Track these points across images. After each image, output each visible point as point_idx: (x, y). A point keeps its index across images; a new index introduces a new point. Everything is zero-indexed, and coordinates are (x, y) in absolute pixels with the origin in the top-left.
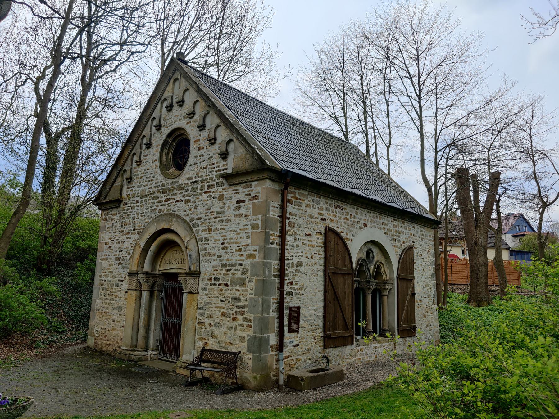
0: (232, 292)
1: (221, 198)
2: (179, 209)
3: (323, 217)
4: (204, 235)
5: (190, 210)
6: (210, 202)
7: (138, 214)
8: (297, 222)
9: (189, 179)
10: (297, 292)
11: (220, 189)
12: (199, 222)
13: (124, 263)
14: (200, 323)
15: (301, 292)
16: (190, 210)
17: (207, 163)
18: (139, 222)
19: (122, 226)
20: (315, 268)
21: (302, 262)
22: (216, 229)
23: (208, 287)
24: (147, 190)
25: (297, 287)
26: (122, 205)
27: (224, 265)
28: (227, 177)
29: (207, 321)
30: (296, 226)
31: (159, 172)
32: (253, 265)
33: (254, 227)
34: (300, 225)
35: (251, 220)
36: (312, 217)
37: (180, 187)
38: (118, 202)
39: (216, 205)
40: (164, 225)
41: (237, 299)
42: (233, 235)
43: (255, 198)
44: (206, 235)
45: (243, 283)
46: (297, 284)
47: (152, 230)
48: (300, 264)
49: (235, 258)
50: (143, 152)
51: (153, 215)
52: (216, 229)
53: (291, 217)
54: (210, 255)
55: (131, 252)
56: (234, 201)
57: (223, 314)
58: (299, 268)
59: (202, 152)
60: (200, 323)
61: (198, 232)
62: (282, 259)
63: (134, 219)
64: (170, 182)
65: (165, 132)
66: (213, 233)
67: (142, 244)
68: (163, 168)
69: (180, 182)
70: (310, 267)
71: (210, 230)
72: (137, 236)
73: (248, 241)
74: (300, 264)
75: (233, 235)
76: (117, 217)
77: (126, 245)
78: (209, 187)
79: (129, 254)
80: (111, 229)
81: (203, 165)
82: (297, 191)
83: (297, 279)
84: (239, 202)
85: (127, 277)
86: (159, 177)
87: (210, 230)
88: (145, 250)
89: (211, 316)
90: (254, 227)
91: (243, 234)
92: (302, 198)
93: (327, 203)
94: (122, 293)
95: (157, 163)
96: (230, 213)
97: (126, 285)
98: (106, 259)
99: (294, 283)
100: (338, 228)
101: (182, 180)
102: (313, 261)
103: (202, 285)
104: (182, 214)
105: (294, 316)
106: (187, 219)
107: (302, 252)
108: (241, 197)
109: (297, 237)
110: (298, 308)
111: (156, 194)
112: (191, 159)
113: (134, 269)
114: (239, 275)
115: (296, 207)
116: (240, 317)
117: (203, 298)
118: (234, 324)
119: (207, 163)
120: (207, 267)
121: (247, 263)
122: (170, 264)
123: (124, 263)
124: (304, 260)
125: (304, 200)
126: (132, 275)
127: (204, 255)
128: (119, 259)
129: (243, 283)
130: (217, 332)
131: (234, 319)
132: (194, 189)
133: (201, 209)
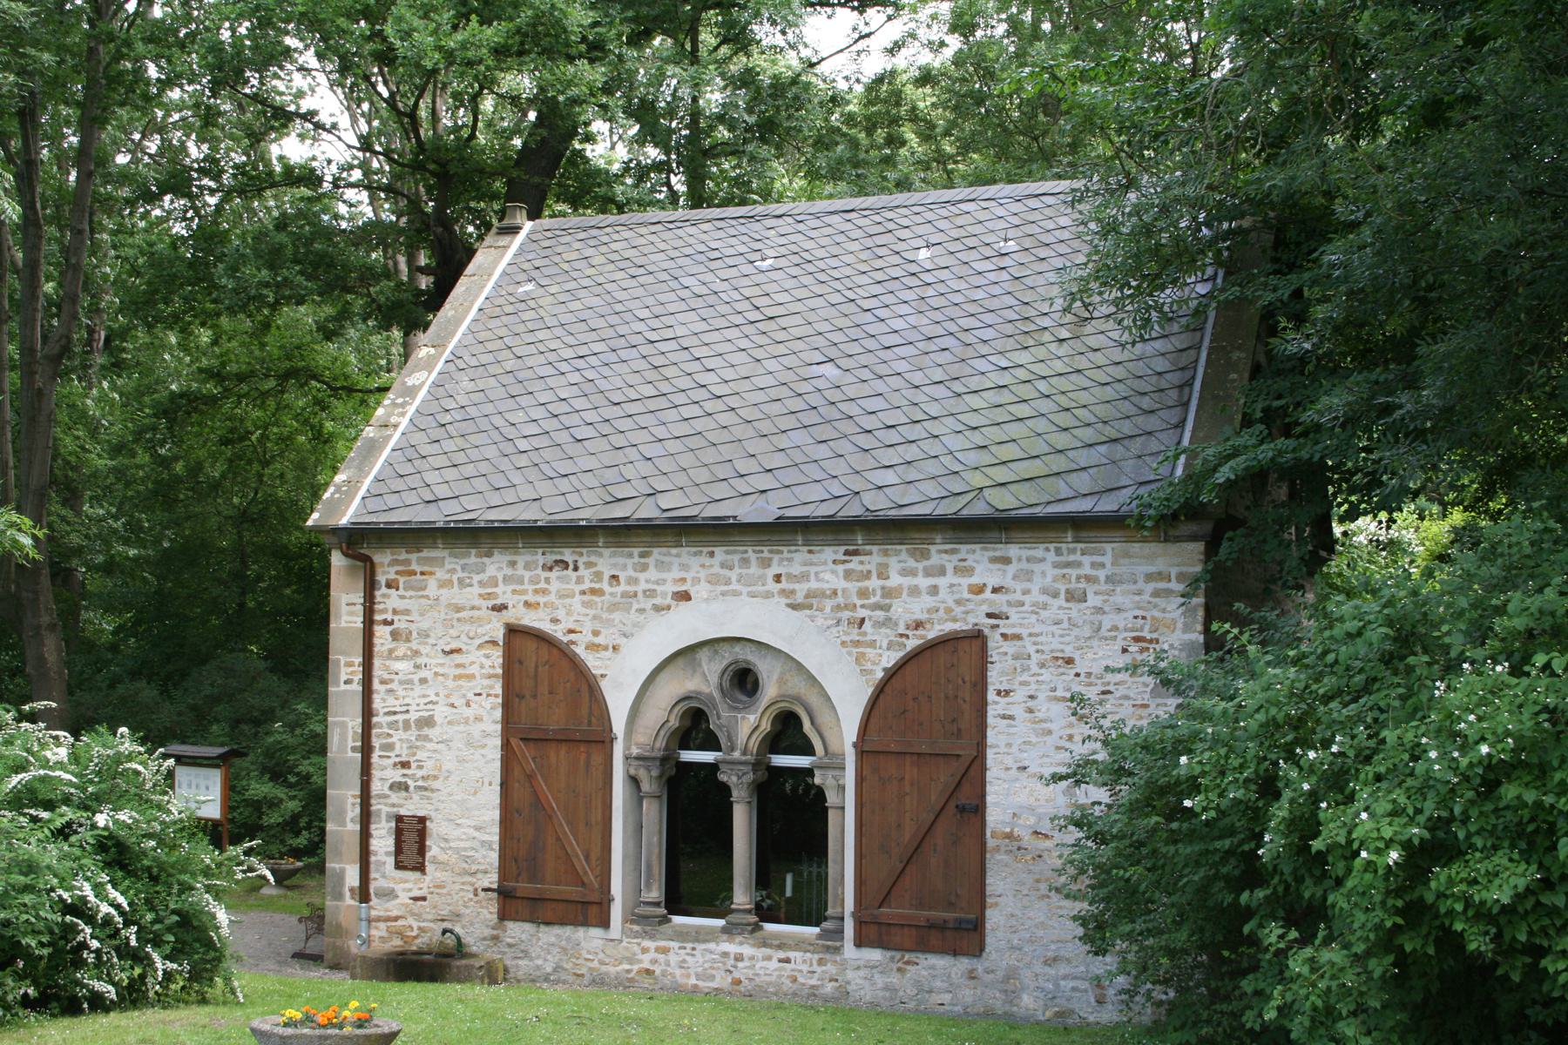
3: (498, 602)
8: (413, 627)
10: (420, 783)
15: (435, 784)
20: (476, 730)
21: (432, 717)
25: (420, 773)
30: (415, 635)
34: (425, 635)
36: (459, 609)
46: (421, 767)
48: (428, 722)
53: (396, 618)
58: (426, 731)
62: (368, 713)
70: (462, 728)
74: (428, 722)
82: (414, 557)
83: (421, 755)
92: (426, 569)
93: (513, 564)
99: (414, 765)
100: (555, 621)
102: (469, 713)
105: (410, 838)
107: (437, 694)
109: (419, 661)
110: (422, 820)
115: (411, 593)
124: (441, 712)
125: (431, 573)
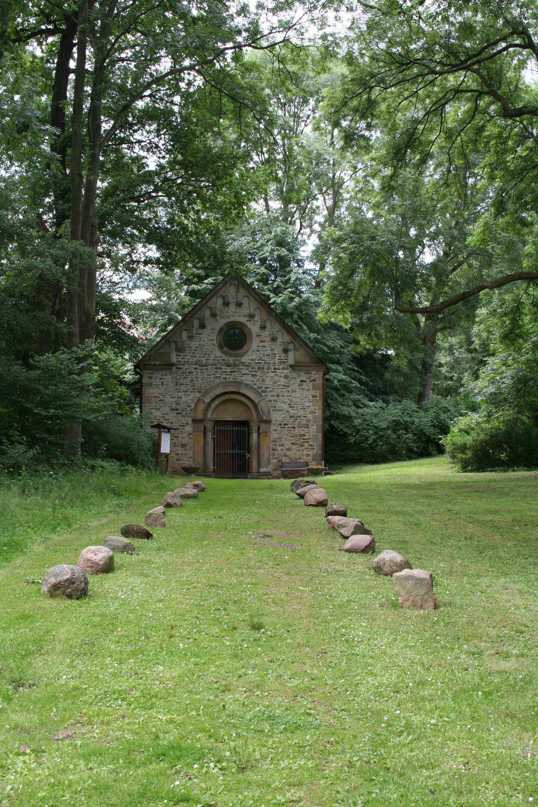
0: (297, 431)
1: (286, 377)
2: (248, 379)
4: (272, 398)
5: (258, 381)
6: (276, 378)
7: (197, 378)
9: (252, 360)
11: (285, 371)
12: (268, 390)
13: (184, 413)
14: (273, 450)
16: (258, 381)
17: (269, 352)
18: (199, 383)
19: (177, 385)
22: (283, 396)
23: (279, 429)
24: (204, 361)
26: (174, 369)
27: (293, 417)
28: (291, 366)
29: (279, 448)
31: (217, 349)
32: (314, 417)
33: (314, 396)
35: (312, 392)
37: (243, 364)
38: (169, 366)
39: (283, 381)
40: (230, 389)
41: (304, 435)
42: (298, 400)
43: (314, 380)
44: (275, 398)
45: (307, 426)
47: (218, 392)
49: (301, 413)
50: (195, 331)
51: (217, 381)
52: (283, 396)
54: (279, 410)
55: (193, 405)
56: (298, 380)
57: (293, 444)
59: (266, 344)
60: (273, 450)
61: (266, 396)
63: (192, 381)
64: (231, 359)
65: (222, 322)
66: (281, 398)
67: (207, 401)
68: (221, 347)
69: (243, 360)
71: (278, 396)
72: (198, 395)
73: (311, 404)
75: (298, 400)
76: (169, 377)
77: (184, 399)
78: (275, 369)
79: (189, 406)
80: (160, 387)
81: (266, 353)
84: (301, 381)
85: (190, 422)
86: (219, 354)
87: (278, 396)
88: (209, 404)
89: (282, 445)
90: (314, 396)
91: (306, 400)
94: (186, 435)
95: (215, 342)
96: (296, 387)
97: (189, 429)
98: (158, 409)
101: (245, 359)
103: (272, 428)
104: (250, 383)
106: (255, 387)
108: (303, 378)
111: (218, 366)
112: (254, 346)
113: (200, 416)
114: (304, 422)
116: (306, 445)
117: (274, 435)
118: (301, 448)
119: (269, 352)
120: (276, 417)
121: (310, 416)
122: (231, 414)
123: (184, 413)
126: (195, 421)
127: (274, 411)
128: (177, 410)
129: (307, 426)
130: (288, 453)
131: (301, 446)
132: (259, 368)
133: (268, 382)
